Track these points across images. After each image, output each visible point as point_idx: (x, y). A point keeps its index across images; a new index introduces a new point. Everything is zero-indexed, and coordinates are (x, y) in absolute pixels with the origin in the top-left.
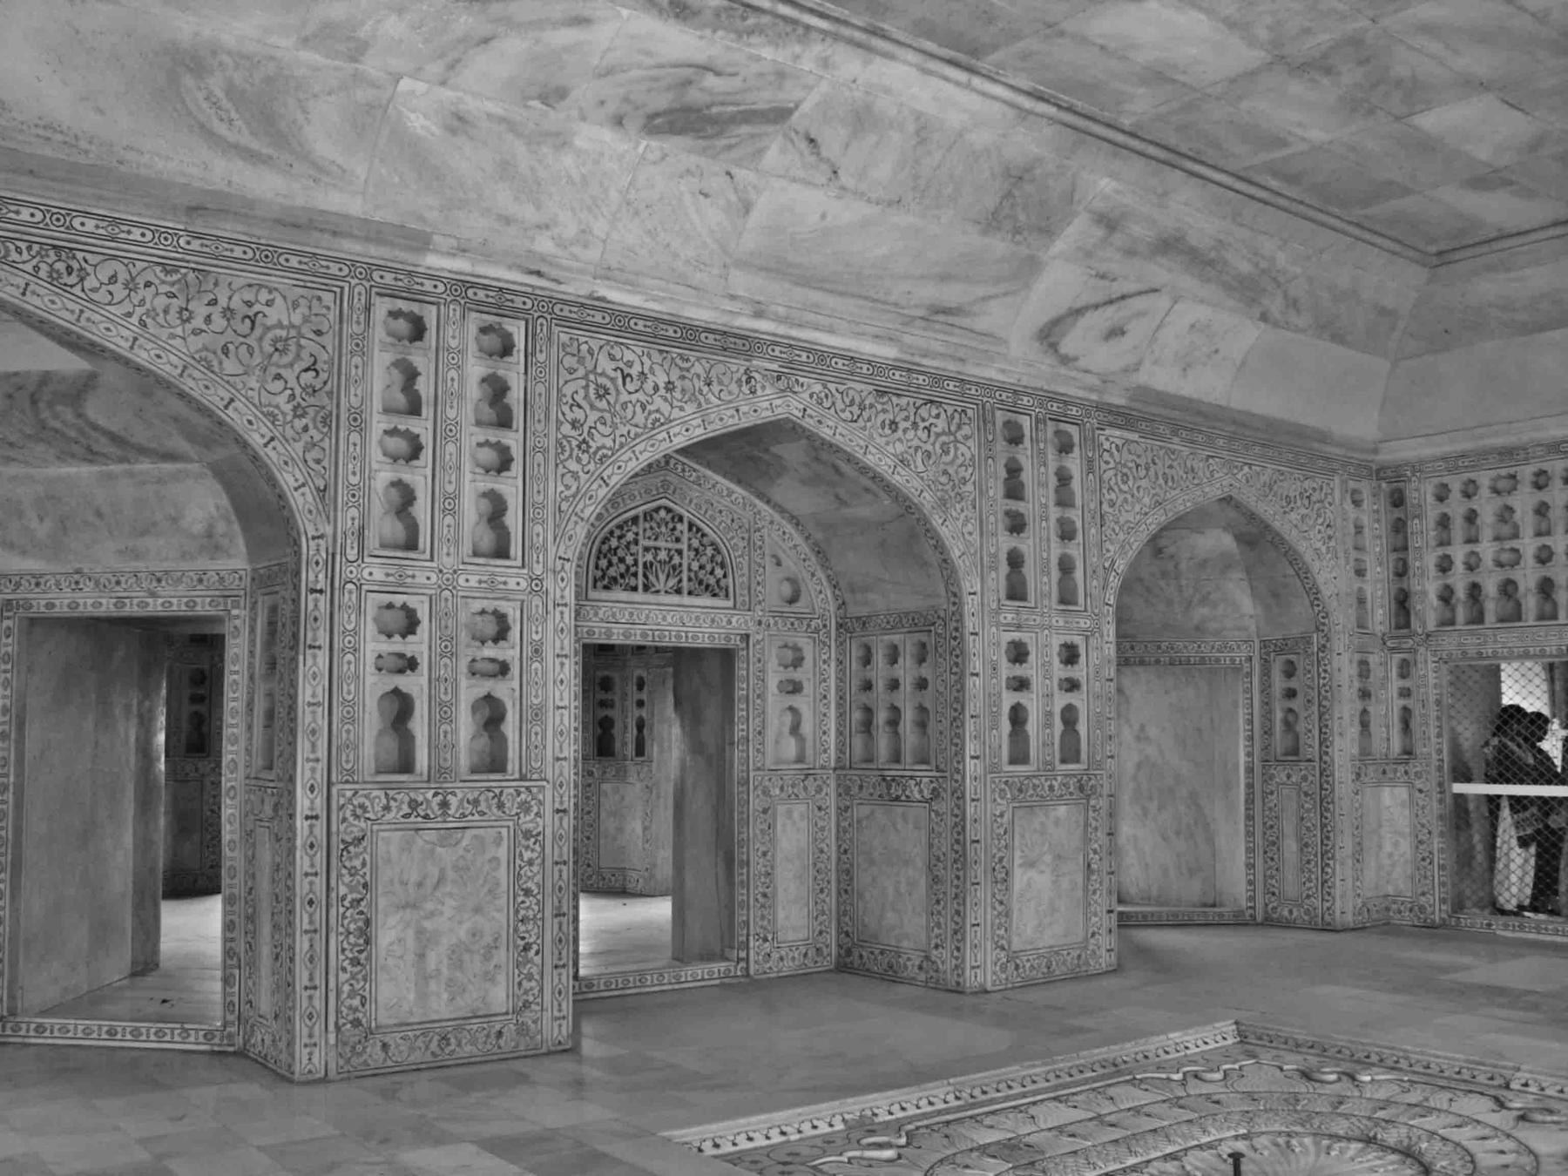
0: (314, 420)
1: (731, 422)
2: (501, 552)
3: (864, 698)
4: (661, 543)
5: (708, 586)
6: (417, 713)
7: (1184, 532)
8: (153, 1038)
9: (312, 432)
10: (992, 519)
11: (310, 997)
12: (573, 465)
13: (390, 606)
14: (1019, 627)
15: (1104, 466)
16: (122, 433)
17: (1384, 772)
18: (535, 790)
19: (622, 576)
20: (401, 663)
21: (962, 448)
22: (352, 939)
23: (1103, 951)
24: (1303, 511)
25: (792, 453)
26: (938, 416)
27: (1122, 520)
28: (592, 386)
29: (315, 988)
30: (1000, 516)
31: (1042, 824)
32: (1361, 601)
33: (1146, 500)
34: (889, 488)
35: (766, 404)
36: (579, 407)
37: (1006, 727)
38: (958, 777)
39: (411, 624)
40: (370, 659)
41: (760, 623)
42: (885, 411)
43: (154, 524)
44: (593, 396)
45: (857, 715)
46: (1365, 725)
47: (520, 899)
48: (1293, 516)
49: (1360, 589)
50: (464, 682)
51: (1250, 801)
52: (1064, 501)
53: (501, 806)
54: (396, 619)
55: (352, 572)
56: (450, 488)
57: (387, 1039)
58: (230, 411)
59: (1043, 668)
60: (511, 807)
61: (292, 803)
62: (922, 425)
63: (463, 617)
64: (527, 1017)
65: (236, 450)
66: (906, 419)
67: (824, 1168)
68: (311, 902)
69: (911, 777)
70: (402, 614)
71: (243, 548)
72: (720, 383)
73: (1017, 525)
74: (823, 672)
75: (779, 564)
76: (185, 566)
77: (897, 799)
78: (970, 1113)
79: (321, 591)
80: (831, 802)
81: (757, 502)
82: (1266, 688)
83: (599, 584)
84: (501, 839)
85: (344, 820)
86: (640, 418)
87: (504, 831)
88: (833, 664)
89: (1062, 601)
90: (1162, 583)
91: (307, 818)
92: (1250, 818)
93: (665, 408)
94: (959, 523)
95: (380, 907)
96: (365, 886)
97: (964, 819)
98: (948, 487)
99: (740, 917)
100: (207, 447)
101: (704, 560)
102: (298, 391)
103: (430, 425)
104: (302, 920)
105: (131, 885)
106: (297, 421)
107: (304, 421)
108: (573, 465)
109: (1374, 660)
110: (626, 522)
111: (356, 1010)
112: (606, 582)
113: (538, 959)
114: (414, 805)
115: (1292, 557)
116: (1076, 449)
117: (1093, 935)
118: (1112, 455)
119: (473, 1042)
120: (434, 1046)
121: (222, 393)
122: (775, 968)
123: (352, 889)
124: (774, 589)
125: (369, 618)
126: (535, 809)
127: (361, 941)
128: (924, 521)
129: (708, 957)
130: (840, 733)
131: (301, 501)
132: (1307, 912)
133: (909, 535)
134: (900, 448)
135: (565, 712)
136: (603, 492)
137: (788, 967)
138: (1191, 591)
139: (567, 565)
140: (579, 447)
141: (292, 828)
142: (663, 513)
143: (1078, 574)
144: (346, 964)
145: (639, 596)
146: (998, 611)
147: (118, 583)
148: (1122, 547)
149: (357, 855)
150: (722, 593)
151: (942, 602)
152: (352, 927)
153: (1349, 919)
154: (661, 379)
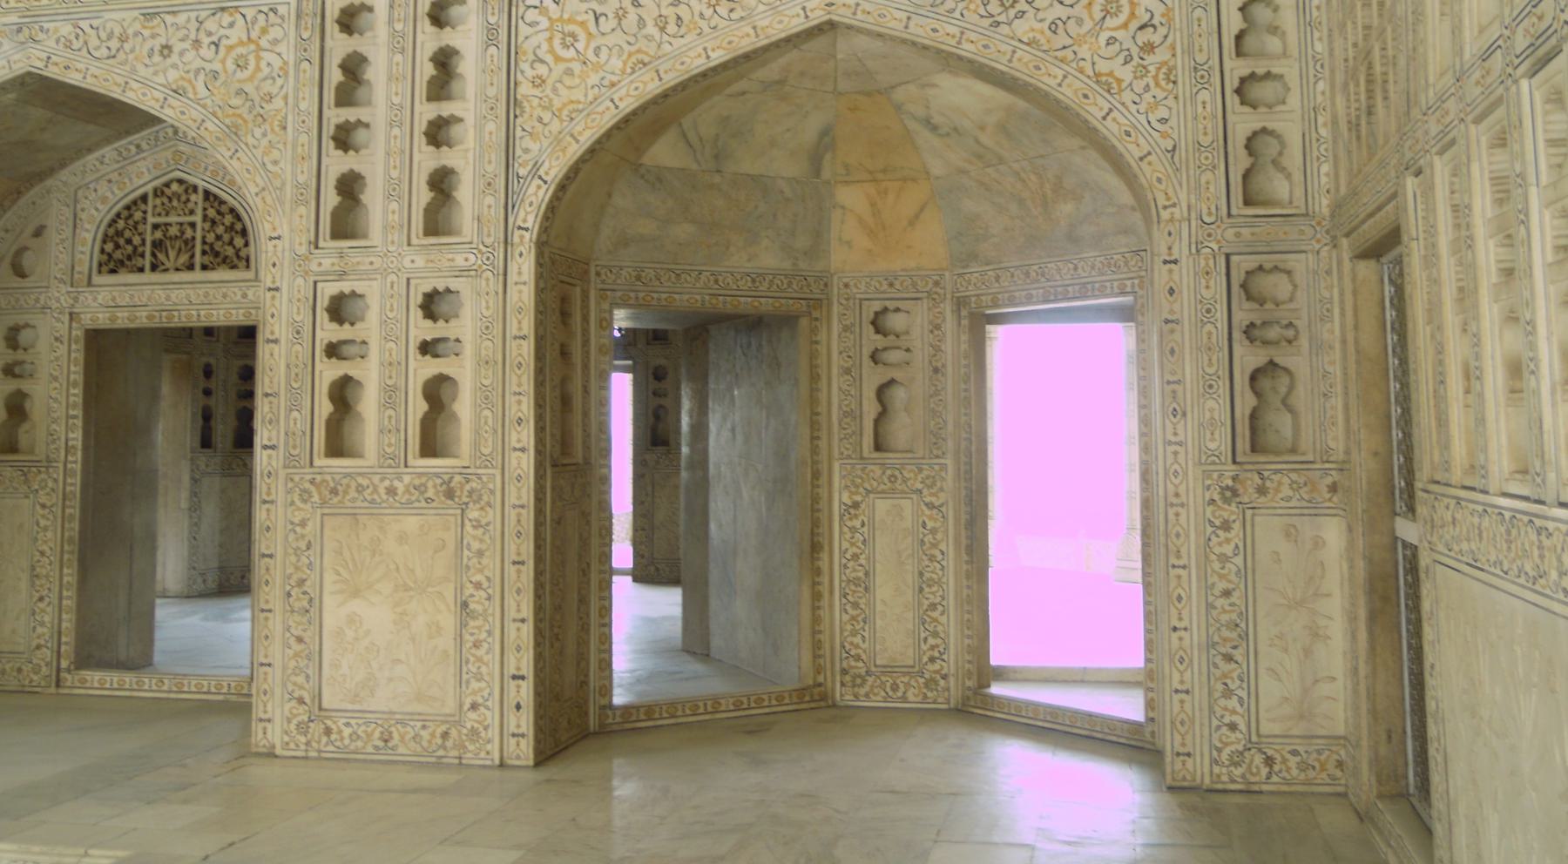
4: (173, 219)
7: (912, 88)
14: (342, 275)
15: (524, 30)
19: (129, 258)
26: (231, 25)
27: (557, 103)
33: (616, 63)
42: (153, 36)
62: (206, 40)
66: (182, 40)
83: (105, 268)
94: (258, 153)
101: (220, 230)
110: (135, 202)
112: (111, 266)
134: (173, 75)
142: (175, 187)
145: (148, 276)
148: (558, 140)
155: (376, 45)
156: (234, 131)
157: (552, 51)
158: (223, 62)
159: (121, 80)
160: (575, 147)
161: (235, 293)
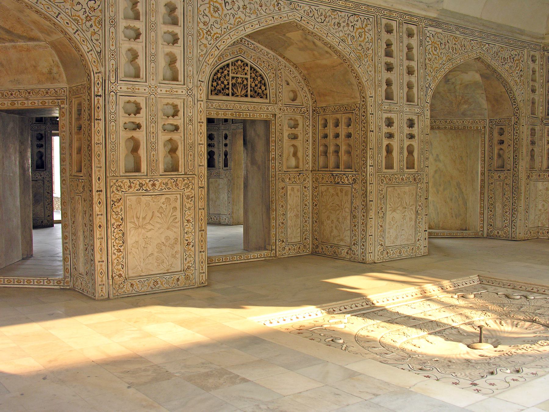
0: (95, 22)
1: (272, 23)
2: (175, 78)
3: (324, 141)
5: (259, 93)
6: (141, 147)
7: (459, 72)
8: (36, 283)
9: (94, 27)
10: (380, 65)
11: (101, 265)
12: (204, 41)
13: (129, 102)
15: (427, 44)
16: (11, 30)
17: (539, 176)
18: (190, 179)
20: (134, 126)
21: (367, 35)
22: (117, 241)
23: (422, 247)
24: (510, 64)
25: (295, 36)
26: (357, 21)
28: (212, 7)
29: (103, 261)
30: (383, 64)
31: (399, 194)
32: (533, 103)
33: (444, 58)
34: (336, 52)
35: (285, 15)
36: (207, 16)
37: (384, 153)
38: (363, 174)
39: (138, 111)
40: (121, 124)
41: (280, 109)
43: (26, 69)
44: (212, 12)
45: (321, 148)
46: (532, 156)
47: (185, 224)
48: (506, 66)
49: (533, 99)
50: (160, 133)
51: (482, 187)
52: (409, 58)
53: (177, 185)
54: (132, 108)
55: (112, 87)
56: (153, 51)
57: (133, 282)
58: (59, 19)
59: (400, 129)
60: (181, 186)
61: (91, 185)
62: (351, 24)
63: (160, 107)
64: (189, 273)
65: (62, 36)
67: (316, 331)
68: (100, 226)
69: (344, 174)
70: (134, 105)
71: (65, 78)
72: (266, 6)
73: (389, 68)
74: (306, 131)
75: (288, 84)
76: (40, 86)
77: (338, 183)
78: (372, 310)
79: (100, 96)
80: (310, 185)
81: (279, 58)
82: (491, 140)
83: (213, 93)
84: (177, 199)
85: (113, 192)
86: (232, 21)
87: (178, 196)
88: (311, 127)
89: (408, 101)
90: (448, 94)
91: (97, 191)
92: (482, 193)
93: (243, 16)
94: (366, 67)
95: (128, 228)
96: (122, 219)
97: (366, 192)
98: (361, 52)
99: (273, 232)
100: (48, 35)
102: (87, 10)
103: (144, 24)
104: (98, 233)
105: (20, 223)
106: (87, 22)
107: (90, 23)
108: (204, 41)
109: (537, 128)
110: (224, 66)
111: (120, 270)
113: (193, 249)
114: (141, 185)
115: (505, 84)
116: (415, 36)
117: (418, 240)
118: (430, 39)
119: (168, 282)
120: (151, 285)
121: (55, 11)
122: (286, 253)
123: (117, 221)
124: (286, 96)
125: (121, 108)
126: (191, 187)
127: (121, 242)
128: (351, 66)
129: (259, 249)
130: (314, 156)
131: (91, 57)
132: (505, 233)
133: (344, 72)
134: (341, 34)
135: (203, 146)
136: (217, 53)
137: (292, 253)
138: (460, 98)
139: (203, 84)
140: (207, 33)
141: (91, 196)
142: (239, 62)
143: (415, 90)
144: (115, 251)
145: (230, 98)
146: (381, 104)
147: (12, 94)
149: (118, 207)
150: (265, 96)
151: (358, 101)
152: (117, 236)
153: (522, 236)
154: (241, 4)
155: (393, 37)
156: (359, 58)
157: (432, 51)
158: (355, 33)
159: (326, 32)
160: (437, 81)
161: (264, 107)
